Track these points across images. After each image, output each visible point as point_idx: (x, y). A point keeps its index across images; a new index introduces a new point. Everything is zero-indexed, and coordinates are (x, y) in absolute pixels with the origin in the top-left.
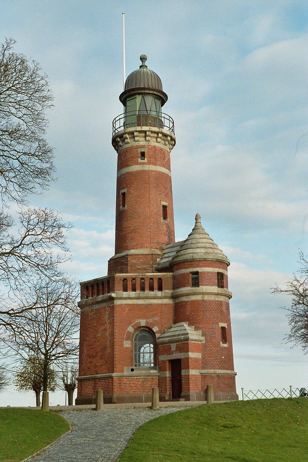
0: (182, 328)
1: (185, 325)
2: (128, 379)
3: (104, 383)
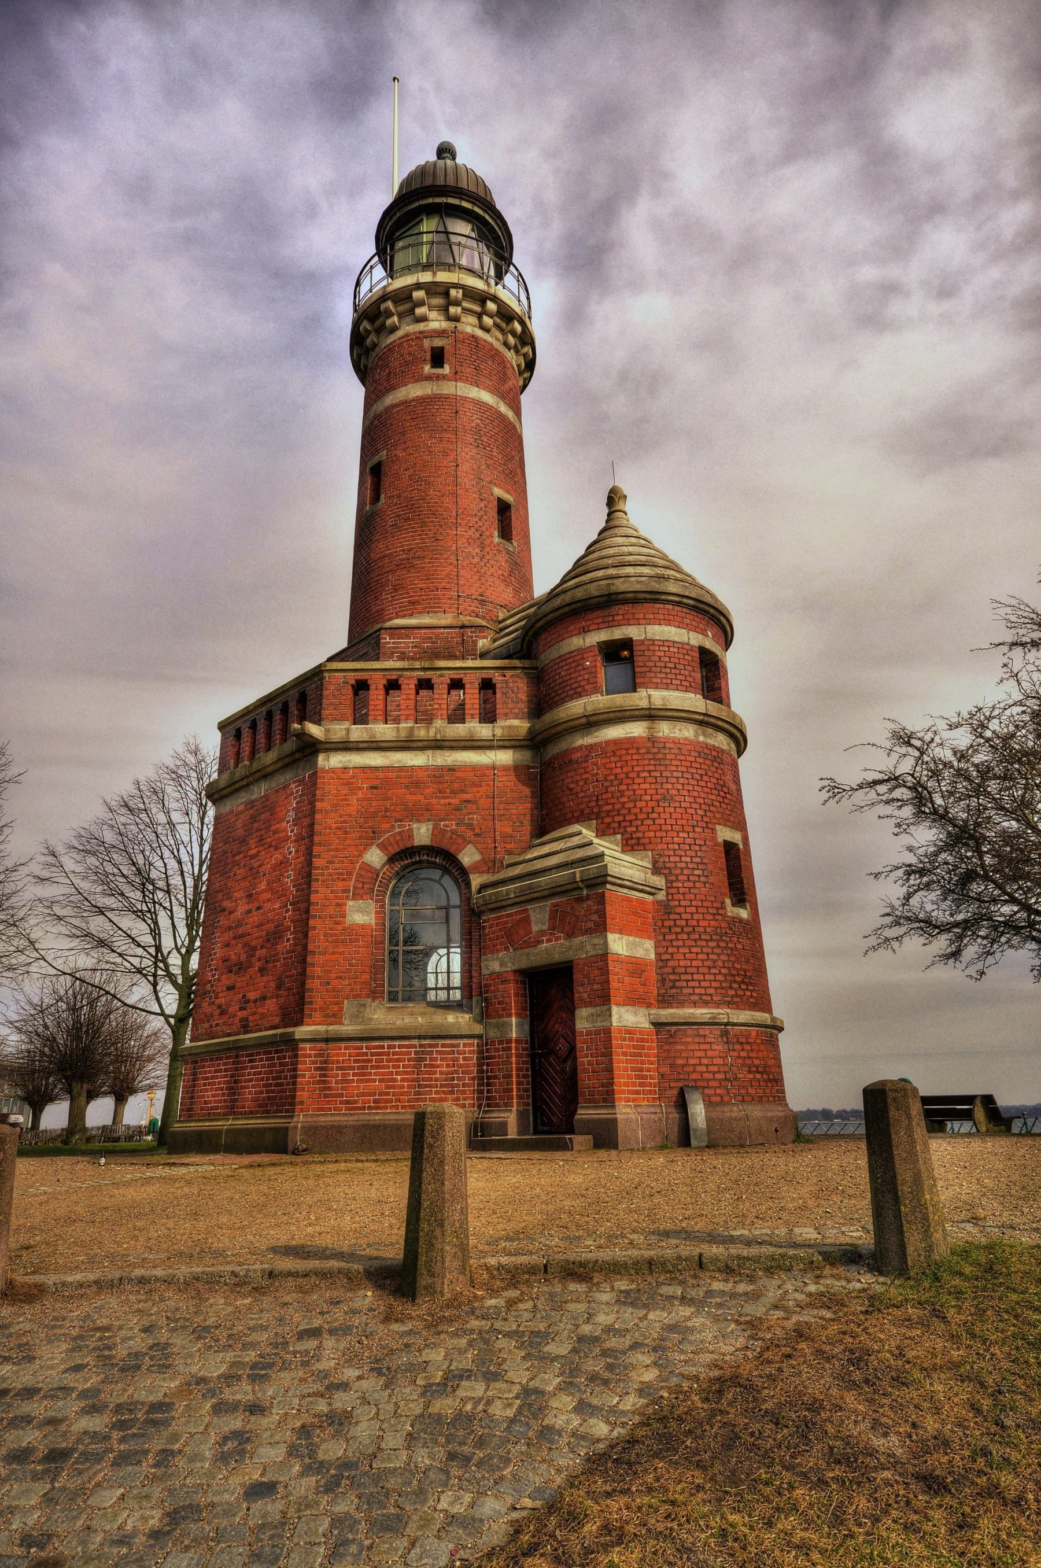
0: (576, 841)
2: (356, 1048)
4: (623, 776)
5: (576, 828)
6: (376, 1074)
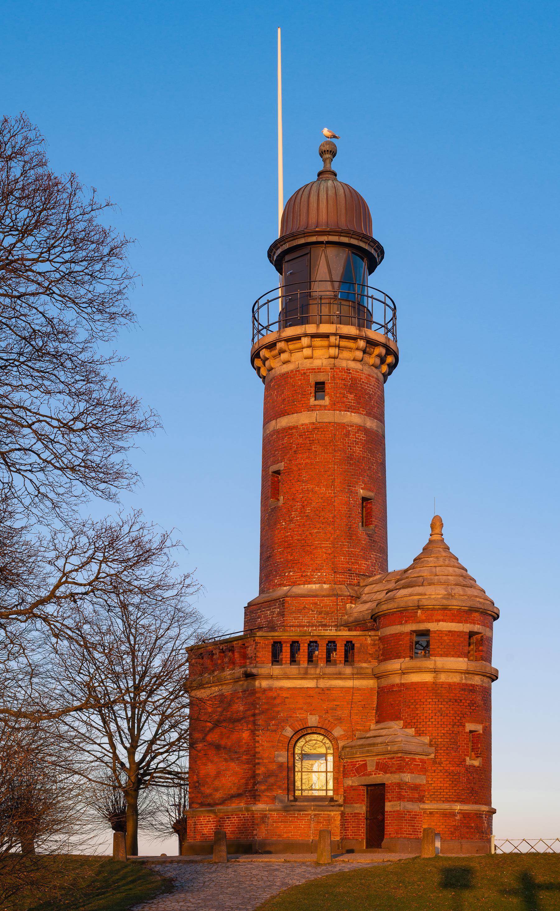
4: (419, 701)
5: (392, 724)
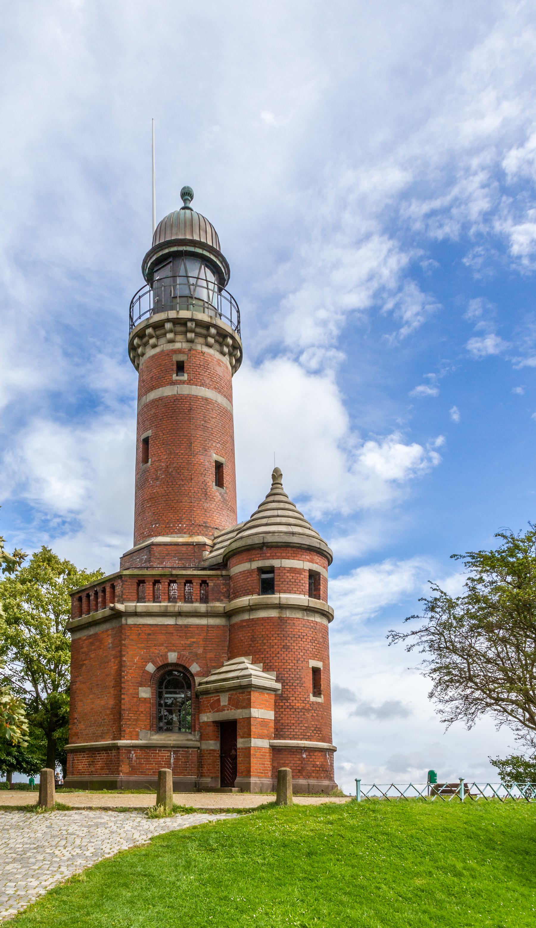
1: (246, 661)
3: (104, 756)
4: (266, 636)
5: (242, 659)
6: (153, 761)
